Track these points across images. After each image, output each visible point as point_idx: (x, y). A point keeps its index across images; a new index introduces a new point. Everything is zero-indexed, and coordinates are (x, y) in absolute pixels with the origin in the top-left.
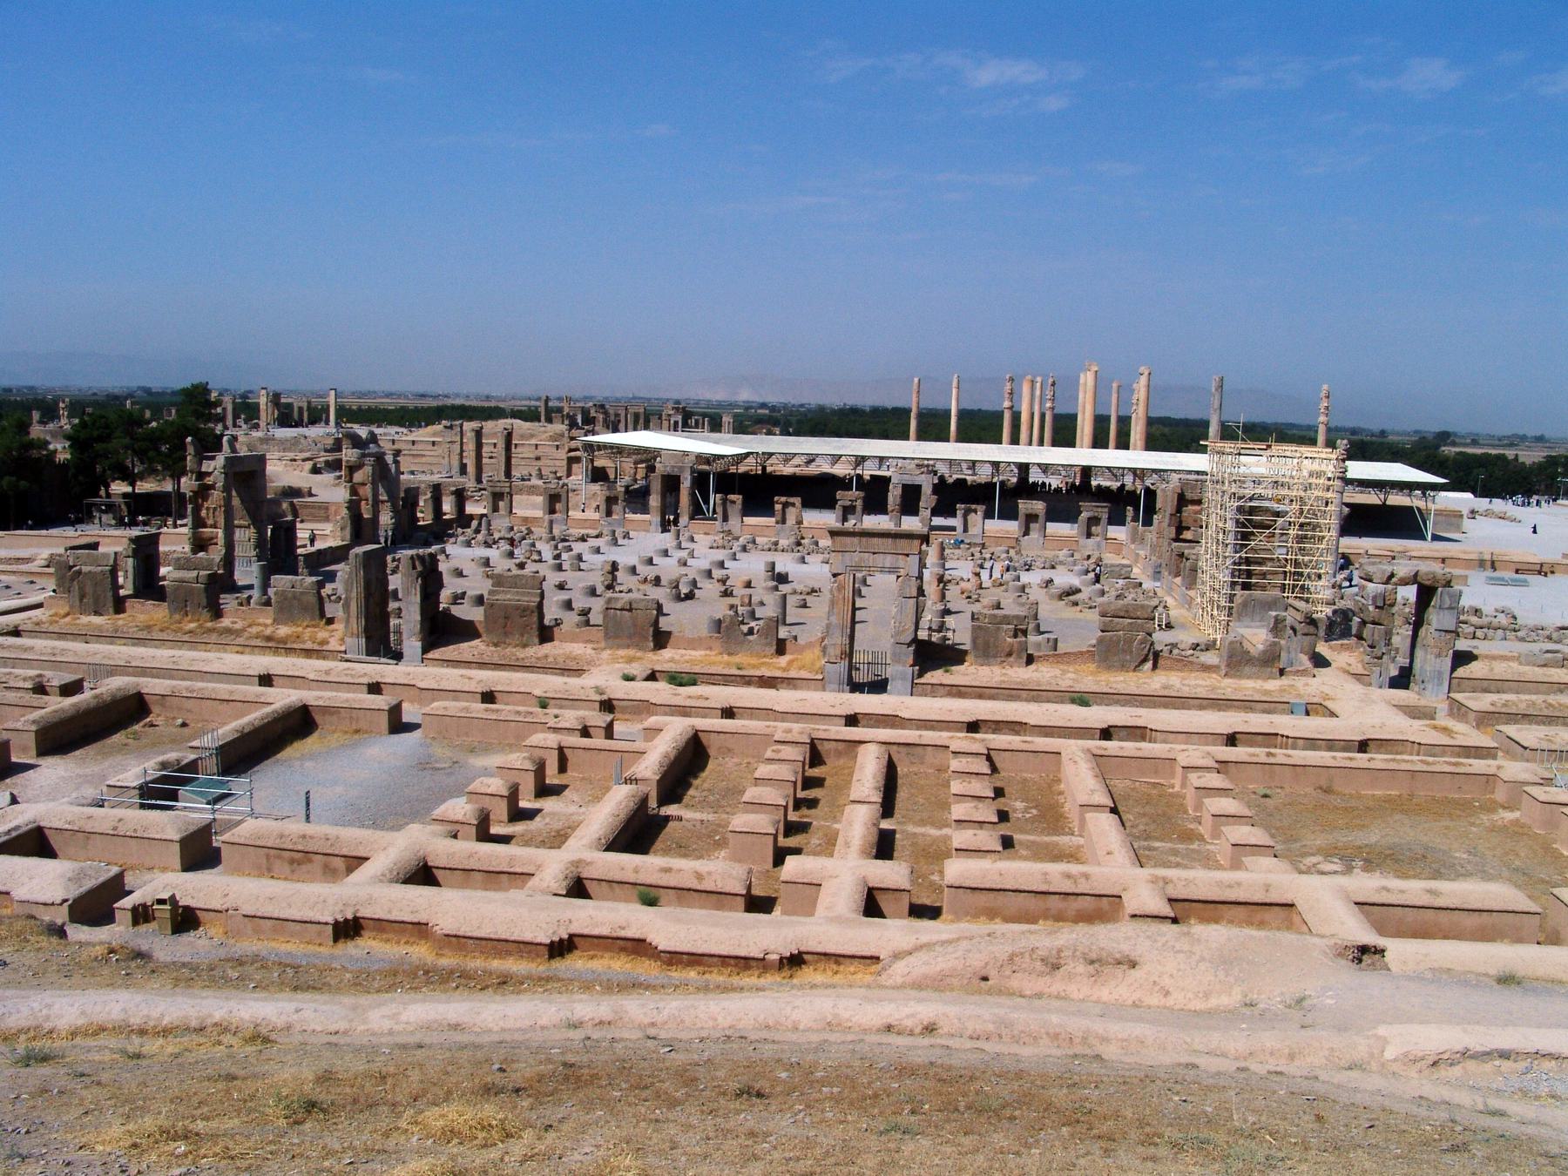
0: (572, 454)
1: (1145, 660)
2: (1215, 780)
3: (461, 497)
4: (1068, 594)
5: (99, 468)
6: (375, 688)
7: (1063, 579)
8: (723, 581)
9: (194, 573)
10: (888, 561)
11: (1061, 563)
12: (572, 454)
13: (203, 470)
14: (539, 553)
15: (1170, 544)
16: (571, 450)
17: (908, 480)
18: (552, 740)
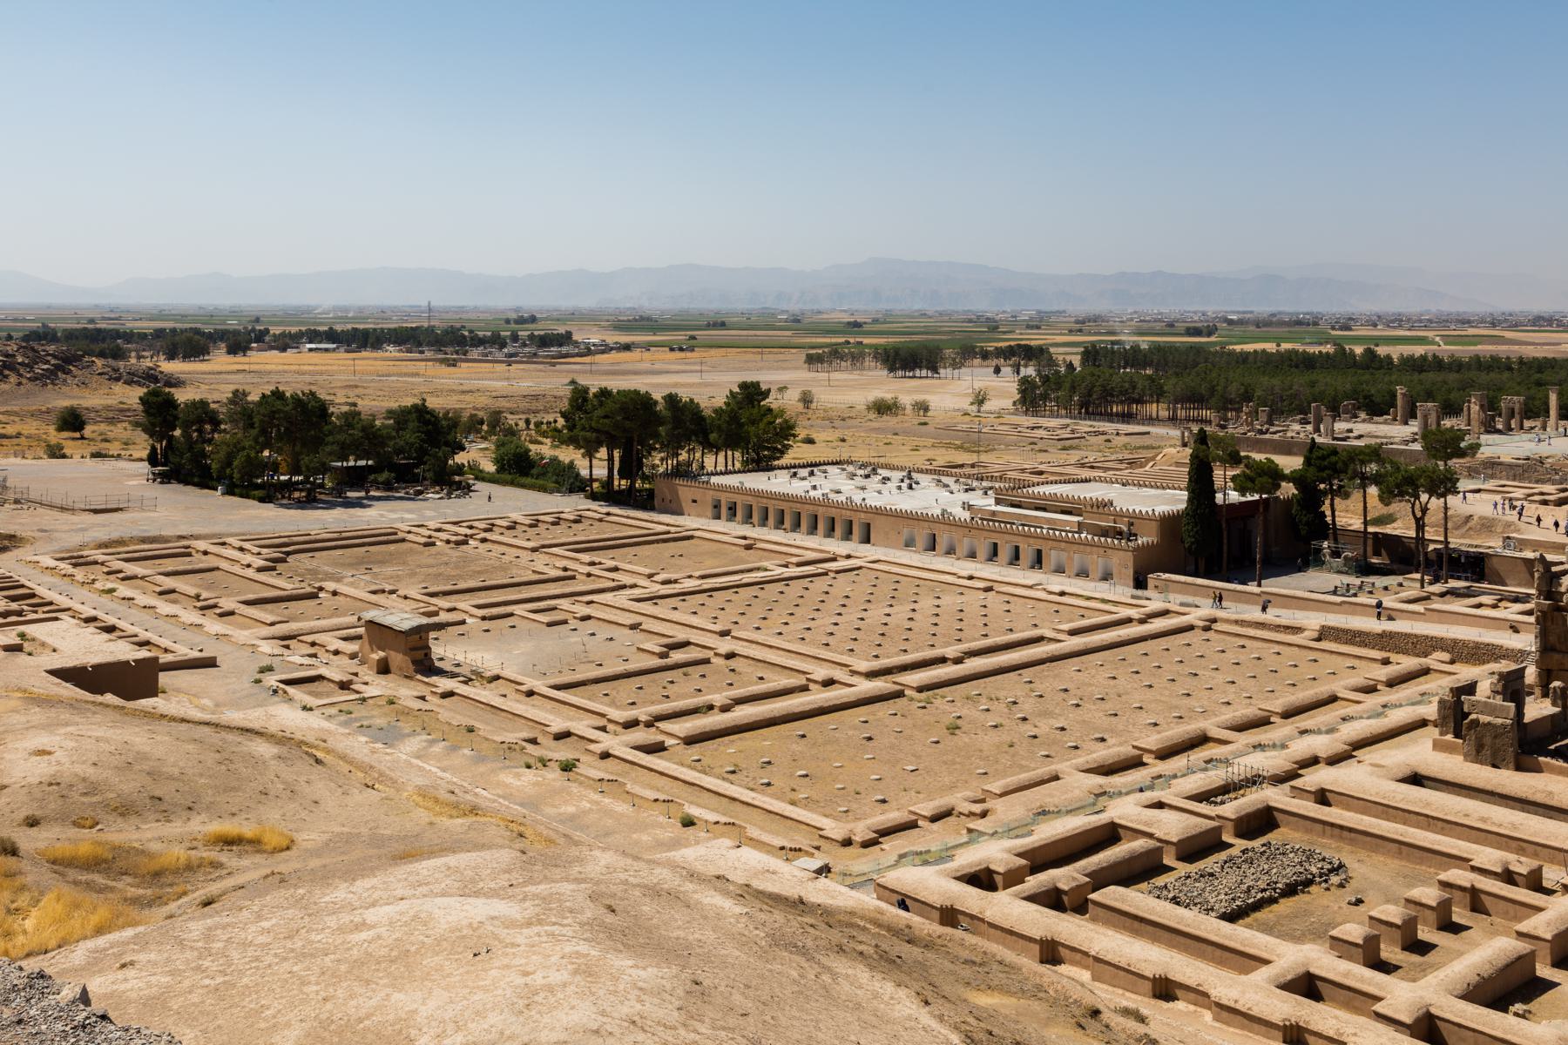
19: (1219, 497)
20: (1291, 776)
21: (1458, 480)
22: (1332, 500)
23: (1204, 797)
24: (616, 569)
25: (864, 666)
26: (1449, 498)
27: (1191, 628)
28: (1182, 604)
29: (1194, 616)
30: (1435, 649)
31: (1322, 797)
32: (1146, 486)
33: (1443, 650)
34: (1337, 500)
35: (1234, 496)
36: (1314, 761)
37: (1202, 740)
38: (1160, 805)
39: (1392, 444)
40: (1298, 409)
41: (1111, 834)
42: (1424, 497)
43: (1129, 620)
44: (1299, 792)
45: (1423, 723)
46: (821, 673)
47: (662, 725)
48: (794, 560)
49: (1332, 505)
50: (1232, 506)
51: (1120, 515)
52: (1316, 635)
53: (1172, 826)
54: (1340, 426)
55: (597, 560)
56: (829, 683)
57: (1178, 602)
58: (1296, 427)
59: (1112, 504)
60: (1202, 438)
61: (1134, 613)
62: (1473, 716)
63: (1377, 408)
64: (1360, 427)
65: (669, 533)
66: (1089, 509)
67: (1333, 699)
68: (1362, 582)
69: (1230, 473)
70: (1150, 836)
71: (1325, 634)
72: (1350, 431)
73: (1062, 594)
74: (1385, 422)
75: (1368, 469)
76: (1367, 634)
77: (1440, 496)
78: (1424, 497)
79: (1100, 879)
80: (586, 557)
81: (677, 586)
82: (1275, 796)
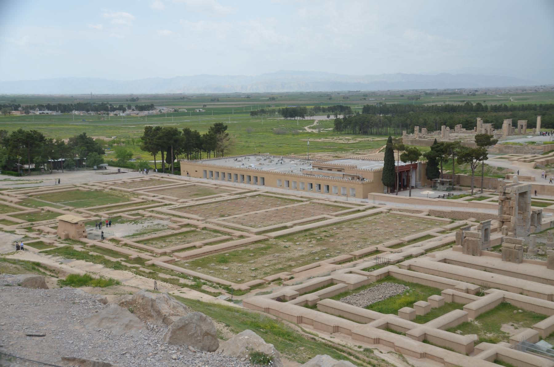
9: (514, 245)
13: (506, 192)
19: (396, 164)
20: (399, 262)
21: (487, 154)
22: (441, 163)
24: (163, 198)
25: (255, 230)
26: (485, 162)
27: (382, 212)
28: (379, 204)
29: (383, 209)
30: (470, 217)
31: (410, 268)
32: (372, 160)
33: (473, 217)
34: (443, 163)
35: (402, 164)
37: (377, 251)
38: (351, 272)
39: (471, 141)
41: (331, 283)
42: (474, 161)
43: (359, 211)
46: (239, 233)
47: (176, 254)
48: (234, 192)
49: (441, 165)
50: (402, 166)
51: (359, 171)
52: (427, 213)
53: (354, 279)
55: (156, 195)
56: (242, 237)
57: (378, 203)
59: (356, 167)
60: (390, 141)
61: (361, 208)
62: (467, 238)
63: (469, 125)
65: (186, 184)
66: (347, 169)
67: (429, 237)
68: (449, 194)
69: (400, 154)
70: (344, 282)
73: (336, 202)
75: (455, 150)
76: (446, 212)
77: (480, 160)
78: (474, 161)
80: (152, 194)
81: (186, 204)
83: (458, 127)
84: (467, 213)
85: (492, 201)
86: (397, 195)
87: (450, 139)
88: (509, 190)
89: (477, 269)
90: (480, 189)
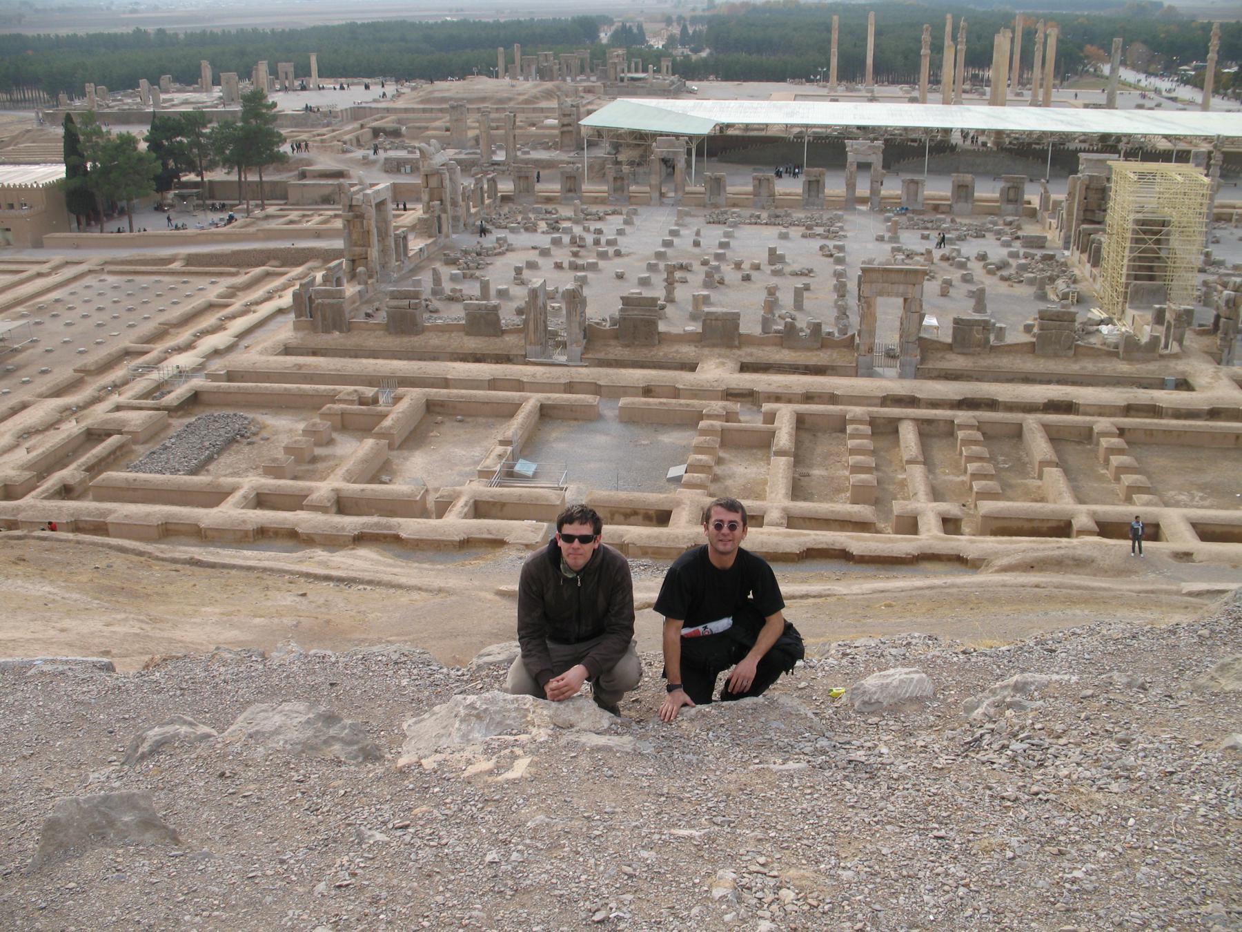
0: (565, 129)
1: (1070, 348)
2: (1116, 441)
3: (493, 182)
4: (999, 268)
5: (171, 164)
6: (570, 387)
7: (997, 252)
8: (738, 266)
9: (406, 302)
10: (901, 288)
11: (989, 230)
12: (565, 129)
13: (354, 203)
14: (582, 239)
15: (1078, 226)
16: (563, 125)
17: (862, 159)
18: (718, 424)
23: (147, 395)
30: (269, 259)
31: (231, 376)
36: (217, 353)
38: (118, 408)
39: (207, 107)
40: (127, 83)
41: (93, 436)
44: (213, 377)
45: (281, 311)
54: (163, 96)
58: (130, 101)
63: (188, 78)
64: (179, 97)
67: (211, 307)
71: (191, 260)
72: (172, 100)
74: (195, 91)
79: (94, 469)
82: (198, 382)
83: (165, 78)
84: (262, 251)
85: (291, 222)
86: (102, 232)
87: (164, 108)
88: (358, 200)
89: (400, 359)
90: (260, 202)
